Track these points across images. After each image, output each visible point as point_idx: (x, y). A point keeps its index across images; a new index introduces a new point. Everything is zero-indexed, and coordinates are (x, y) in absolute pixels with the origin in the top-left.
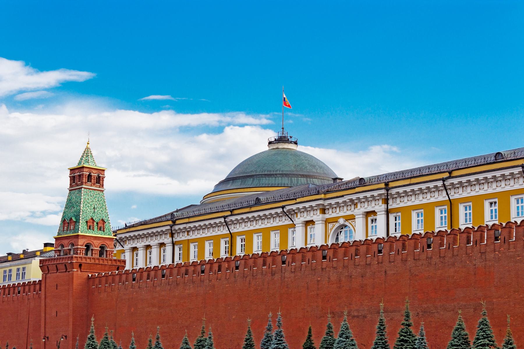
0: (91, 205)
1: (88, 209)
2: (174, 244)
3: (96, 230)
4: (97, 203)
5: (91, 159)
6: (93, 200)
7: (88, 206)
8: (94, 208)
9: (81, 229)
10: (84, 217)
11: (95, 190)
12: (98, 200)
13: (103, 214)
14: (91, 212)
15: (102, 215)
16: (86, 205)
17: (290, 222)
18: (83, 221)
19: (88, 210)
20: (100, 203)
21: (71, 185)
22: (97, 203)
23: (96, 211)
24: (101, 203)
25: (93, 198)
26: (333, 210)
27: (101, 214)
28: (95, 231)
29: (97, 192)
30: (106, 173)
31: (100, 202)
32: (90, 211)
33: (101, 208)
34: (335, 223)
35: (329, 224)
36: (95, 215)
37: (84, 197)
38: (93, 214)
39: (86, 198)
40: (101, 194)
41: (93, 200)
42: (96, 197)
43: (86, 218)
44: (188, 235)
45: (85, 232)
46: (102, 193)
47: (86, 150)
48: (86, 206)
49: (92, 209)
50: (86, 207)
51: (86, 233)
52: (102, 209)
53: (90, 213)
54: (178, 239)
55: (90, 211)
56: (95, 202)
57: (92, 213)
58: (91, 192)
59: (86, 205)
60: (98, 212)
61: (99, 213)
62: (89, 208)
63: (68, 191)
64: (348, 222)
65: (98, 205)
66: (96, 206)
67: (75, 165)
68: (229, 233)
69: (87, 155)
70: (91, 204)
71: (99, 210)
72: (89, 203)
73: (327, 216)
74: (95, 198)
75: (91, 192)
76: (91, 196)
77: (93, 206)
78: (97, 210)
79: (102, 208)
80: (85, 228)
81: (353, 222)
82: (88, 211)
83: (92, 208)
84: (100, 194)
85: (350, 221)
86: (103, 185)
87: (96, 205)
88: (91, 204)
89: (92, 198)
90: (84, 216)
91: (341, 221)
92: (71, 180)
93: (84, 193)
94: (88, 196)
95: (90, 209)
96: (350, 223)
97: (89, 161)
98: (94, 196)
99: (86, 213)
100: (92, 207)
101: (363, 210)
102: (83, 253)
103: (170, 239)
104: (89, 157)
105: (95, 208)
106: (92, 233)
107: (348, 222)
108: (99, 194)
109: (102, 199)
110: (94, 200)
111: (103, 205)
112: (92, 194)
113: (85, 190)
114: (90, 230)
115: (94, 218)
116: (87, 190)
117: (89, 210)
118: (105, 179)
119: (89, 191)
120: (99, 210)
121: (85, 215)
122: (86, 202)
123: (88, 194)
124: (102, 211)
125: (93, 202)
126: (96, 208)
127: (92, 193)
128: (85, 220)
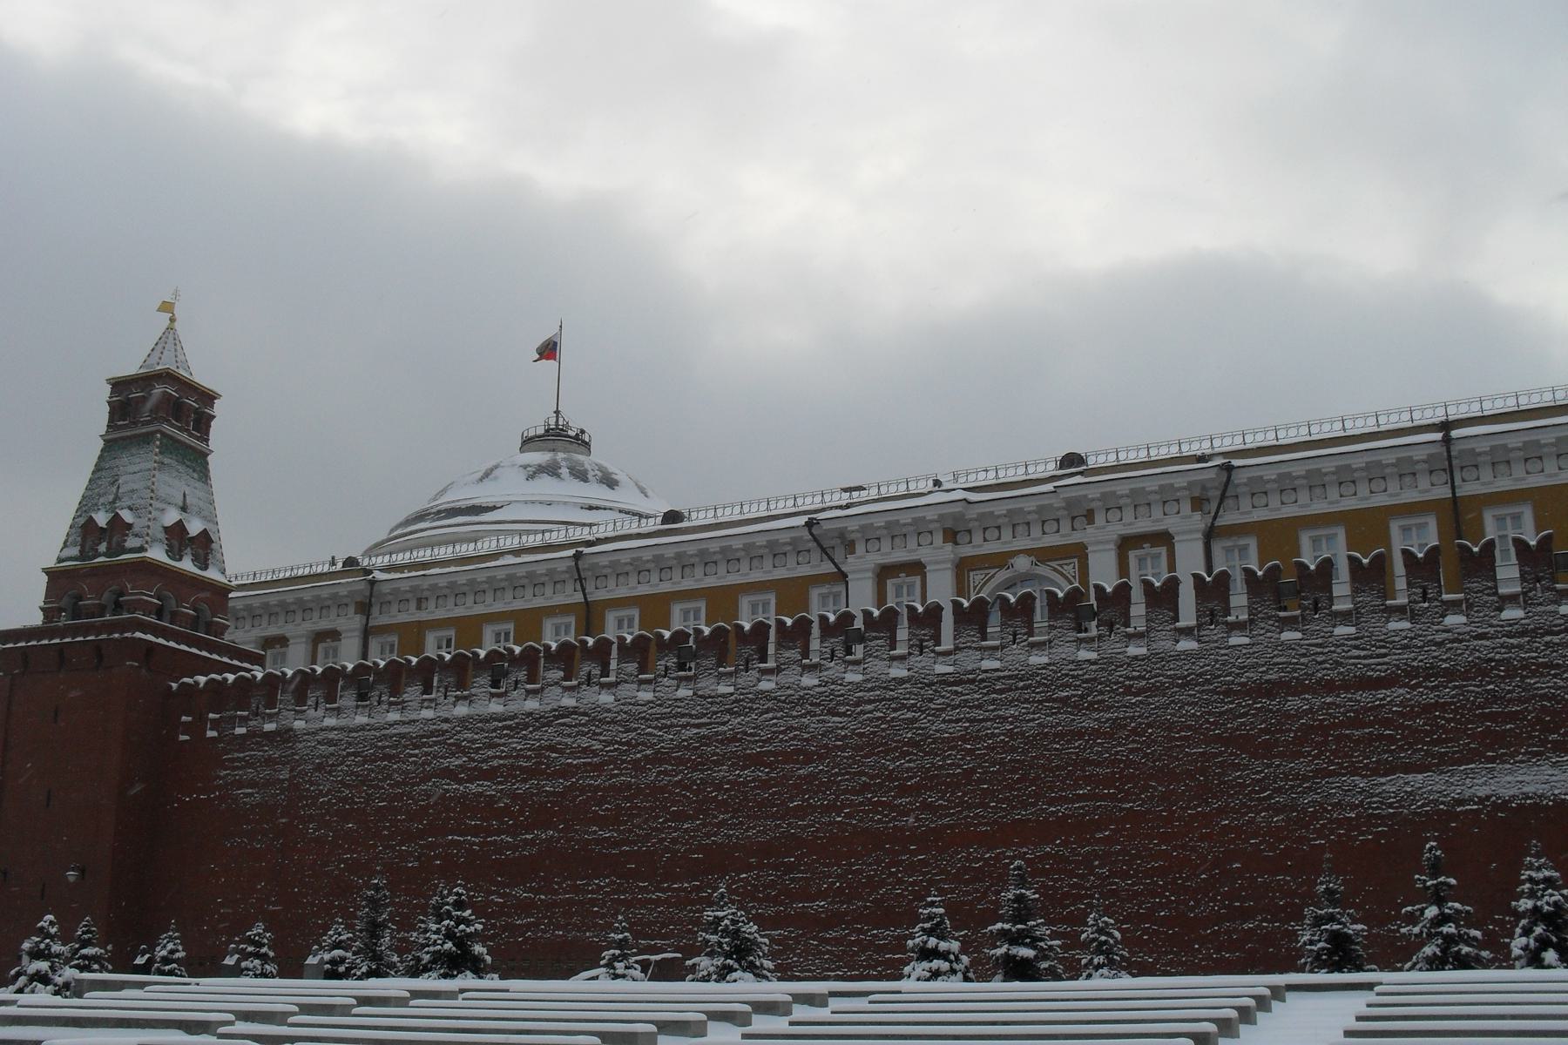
2: (367, 633)
17: (828, 567)
21: (112, 425)
26: (988, 535)
34: (993, 571)
35: (971, 574)
44: (419, 608)
54: (383, 620)
63: (101, 444)
64: (1048, 566)
67: (130, 366)
68: (583, 600)
73: (966, 551)
81: (1065, 567)
85: (1054, 564)
86: (207, 440)
91: (1022, 564)
92: (111, 413)
96: (1055, 570)
101: (1118, 529)
103: (357, 621)
107: (1048, 566)
113: (164, 441)
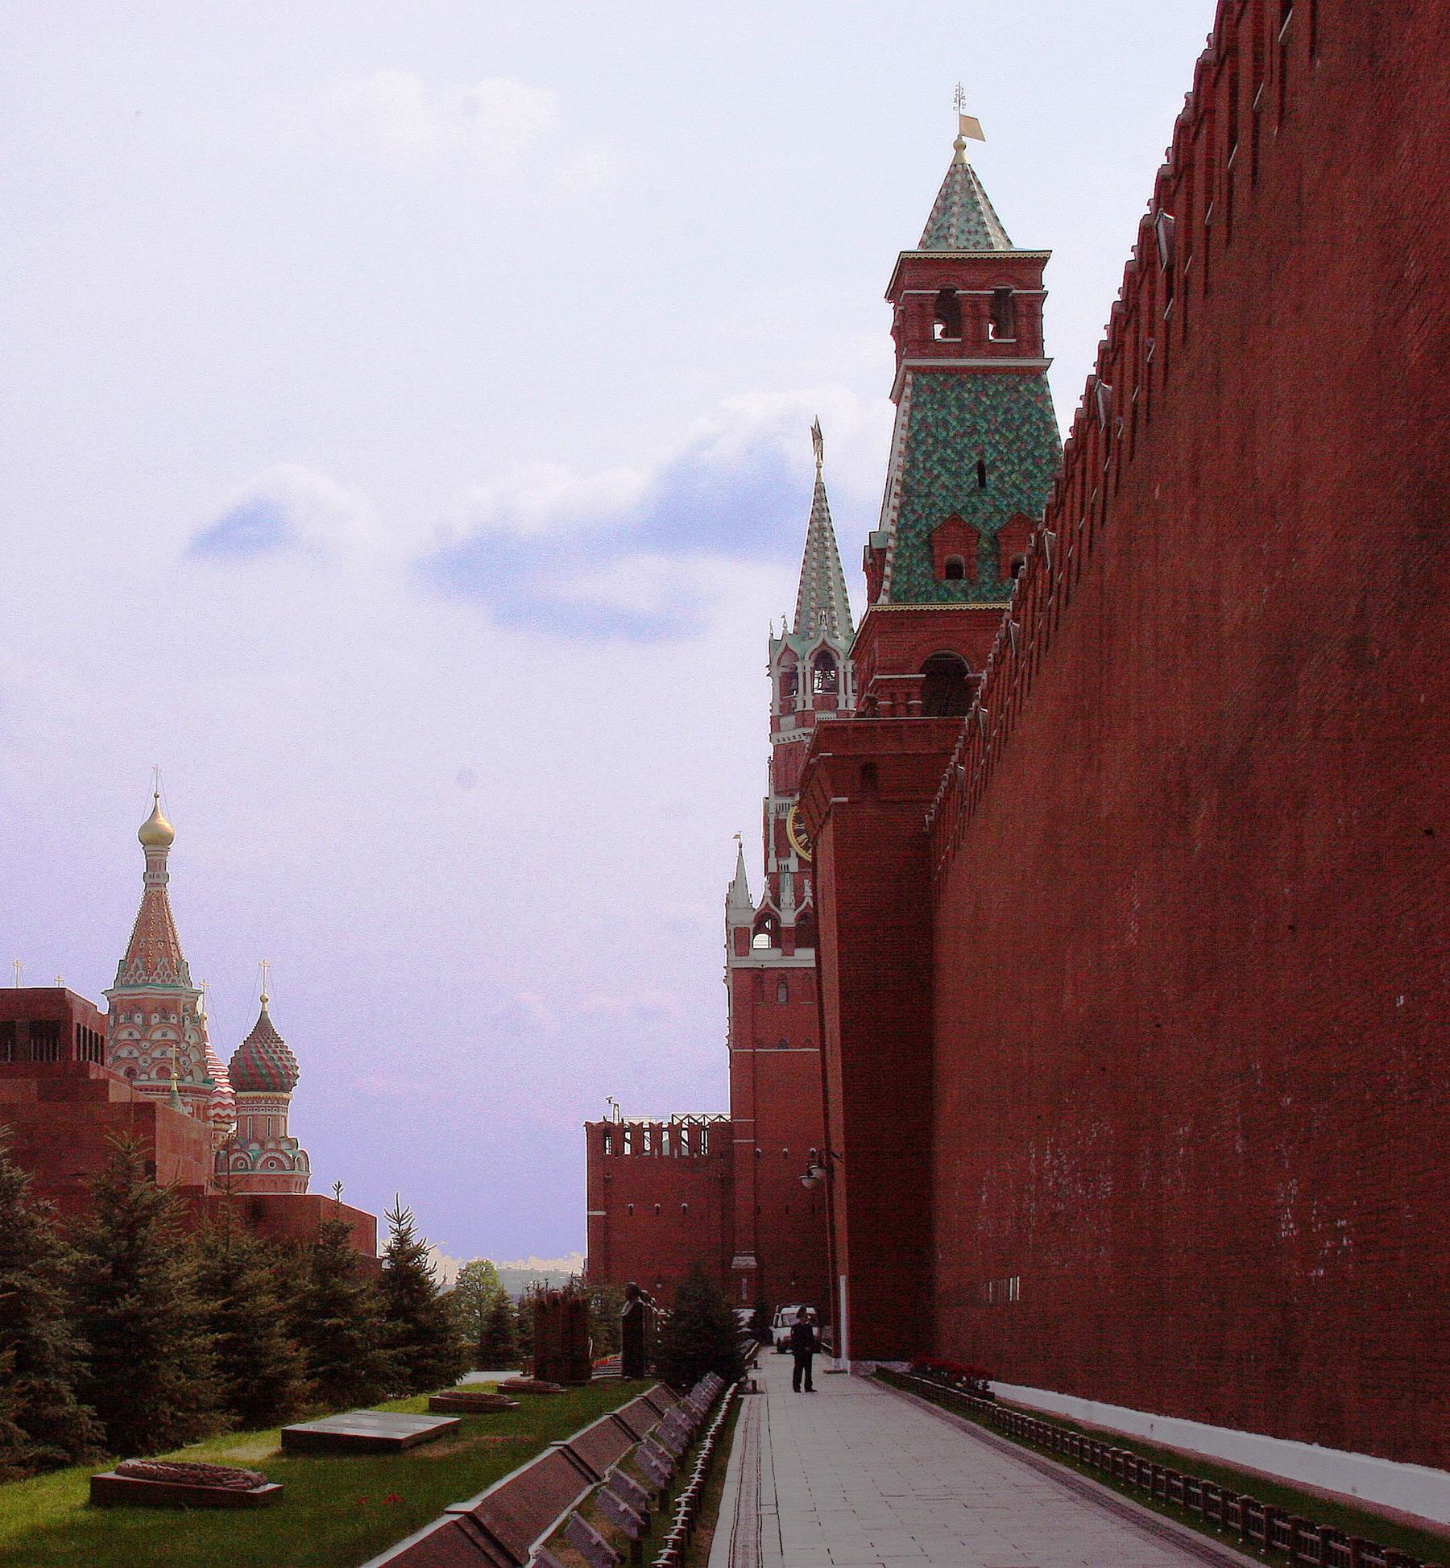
0: (960, 454)
1: (938, 476)
3: (991, 577)
4: (1002, 435)
5: (968, 220)
6: (974, 424)
7: (942, 461)
8: (981, 468)
9: (893, 584)
10: (912, 517)
11: (986, 371)
12: (1007, 423)
13: (1040, 488)
14: (959, 486)
15: (1029, 497)
16: (928, 455)
18: (907, 538)
19: (942, 478)
20: (1018, 438)
22: (1002, 435)
23: (991, 478)
24: (1028, 433)
25: (974, 416)
27: (1021, 491)
28: (984, 583)
29: (1000, 382)
30: (1050, 277)
31: (1018, 428)
32: (950, 483)
33: (1022, 460)
36: (983, 502)
37: (919, 417)
38: (969, 495)
39: (930, 420)
40: (1028, 389)
41: (974, 424)
42: (992, 407)
43: (927, 525)
45: (916, 595)
46: (1031, 385)
47: (958, 177)
48: (925, 461)
49: (968, 474)
50: (928, 465)
51: (928, 600)
52: (1028, 465)
53: (955, 496)
55: (950, 483)
56: (987, 432)
57: (965, 492)
58: (962, 384)
59: (928, 455)
60: (1003, 482)
61: (1014, 485)
62: (948, 470)
65: (1009, 445)
66: (990, 456)
69: (948, 203)
70: (959, 447)
71: (1012, 472)
72: (946, 444)
74: (984, 413)
75: (962, 384)
76: (961, 408)
77: (971, 457)
78: (996, 474)
79: (1030, 461)
80: (923, 575)
82: (944, 486)
83: (968, 464)
84: (1021, 388)
86: (1034, 343)
87: (994, 446)
88: (959, 447)
89: (968, 416)
90: (913, 511)
93: (919, 396)
94: (942, 406)
95: (955, 475)
97: (953, 230)
98: (981, 402)
99: (928, 495)
100: (966, 461)
102: (908, 706)
104: (955, 209)
105: (987, 462)
106: (966, 594)
108: (1018, 391)
109: (1030, 415)
110: (983, 425)
111: (1038, 444)
112: (966, 396)
114: (948, 583)
115: (978, 520)
116: (936, 380)
117: (945, 478)
118: (1047, 308)
119: (952, 381)
120: (1012, 472)
121: (923, 506)
122: (930, 441)
123: (944, 399)
124: (1028, 475)
125: (976, 437)
126: (993, 462)
127: (970, 391)
128: (918, 535)
